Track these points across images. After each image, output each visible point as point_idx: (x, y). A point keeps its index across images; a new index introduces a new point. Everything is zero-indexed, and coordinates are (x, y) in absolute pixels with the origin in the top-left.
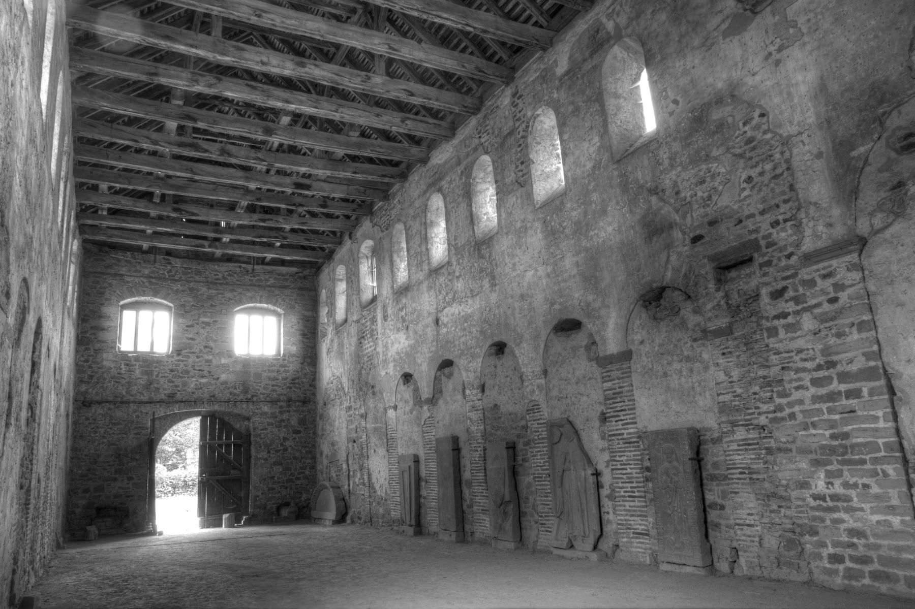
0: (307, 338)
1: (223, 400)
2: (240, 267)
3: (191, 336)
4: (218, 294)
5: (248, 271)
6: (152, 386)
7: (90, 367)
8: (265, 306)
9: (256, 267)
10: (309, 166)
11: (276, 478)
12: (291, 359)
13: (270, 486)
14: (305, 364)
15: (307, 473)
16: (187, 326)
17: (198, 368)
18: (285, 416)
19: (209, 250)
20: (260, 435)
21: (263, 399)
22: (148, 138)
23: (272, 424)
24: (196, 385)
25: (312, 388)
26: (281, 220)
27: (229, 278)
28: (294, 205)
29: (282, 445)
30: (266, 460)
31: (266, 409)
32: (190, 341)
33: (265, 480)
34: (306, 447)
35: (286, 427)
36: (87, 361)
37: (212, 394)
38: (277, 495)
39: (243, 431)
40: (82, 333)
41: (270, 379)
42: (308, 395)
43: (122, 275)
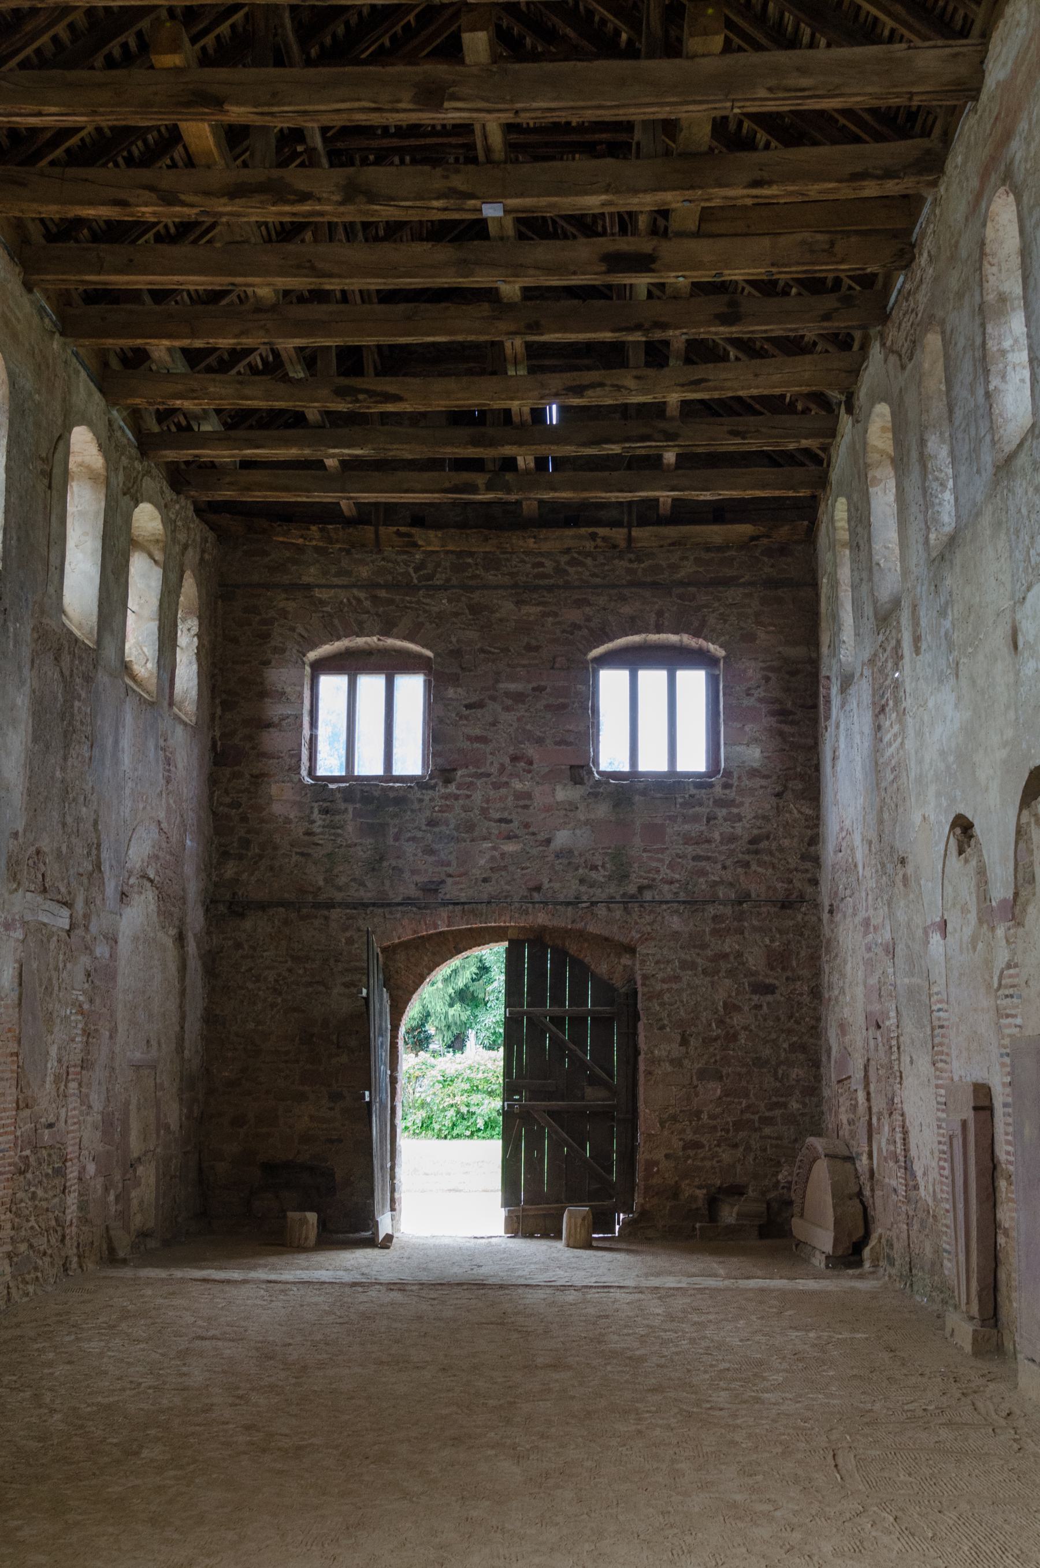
0: (792, 723)
1: (561, 898)
2: (593, 536)
3: (478, 732)
4: (544, 615)
5: (615, 547)
6: (385, 864)
7: (244, 819)
8: (673, 638)
9: (636, 532)
10: (606, 191)
12: (746, 783)
13: (689, 1136)
14: (789, 795)
15: (794, 1105)
16: (468, 707)
17: (498, 816)
18: (729, 944)
19: (490, 496)
20: (660, 994)
21: (669, 897)
22: (151, 188)
23: (693, 966)
24: (493, 858)
25: (808, 865)
26: (630, 383)
27: (571, 570)
28: (638, 327)
29: (721, 1022)
30: (676, 1062)
31: (675, 923)
32: (476, 745)
33: (674, 1118)
34: (790, 1032)
35: (731, 973)
36: (235, 805)
37: (531, 884)
38: (708, 1164)
39: (618, 982)
40: (223, 735)
41: (688, 840)
42: (798, 884)
43: (308, 587)
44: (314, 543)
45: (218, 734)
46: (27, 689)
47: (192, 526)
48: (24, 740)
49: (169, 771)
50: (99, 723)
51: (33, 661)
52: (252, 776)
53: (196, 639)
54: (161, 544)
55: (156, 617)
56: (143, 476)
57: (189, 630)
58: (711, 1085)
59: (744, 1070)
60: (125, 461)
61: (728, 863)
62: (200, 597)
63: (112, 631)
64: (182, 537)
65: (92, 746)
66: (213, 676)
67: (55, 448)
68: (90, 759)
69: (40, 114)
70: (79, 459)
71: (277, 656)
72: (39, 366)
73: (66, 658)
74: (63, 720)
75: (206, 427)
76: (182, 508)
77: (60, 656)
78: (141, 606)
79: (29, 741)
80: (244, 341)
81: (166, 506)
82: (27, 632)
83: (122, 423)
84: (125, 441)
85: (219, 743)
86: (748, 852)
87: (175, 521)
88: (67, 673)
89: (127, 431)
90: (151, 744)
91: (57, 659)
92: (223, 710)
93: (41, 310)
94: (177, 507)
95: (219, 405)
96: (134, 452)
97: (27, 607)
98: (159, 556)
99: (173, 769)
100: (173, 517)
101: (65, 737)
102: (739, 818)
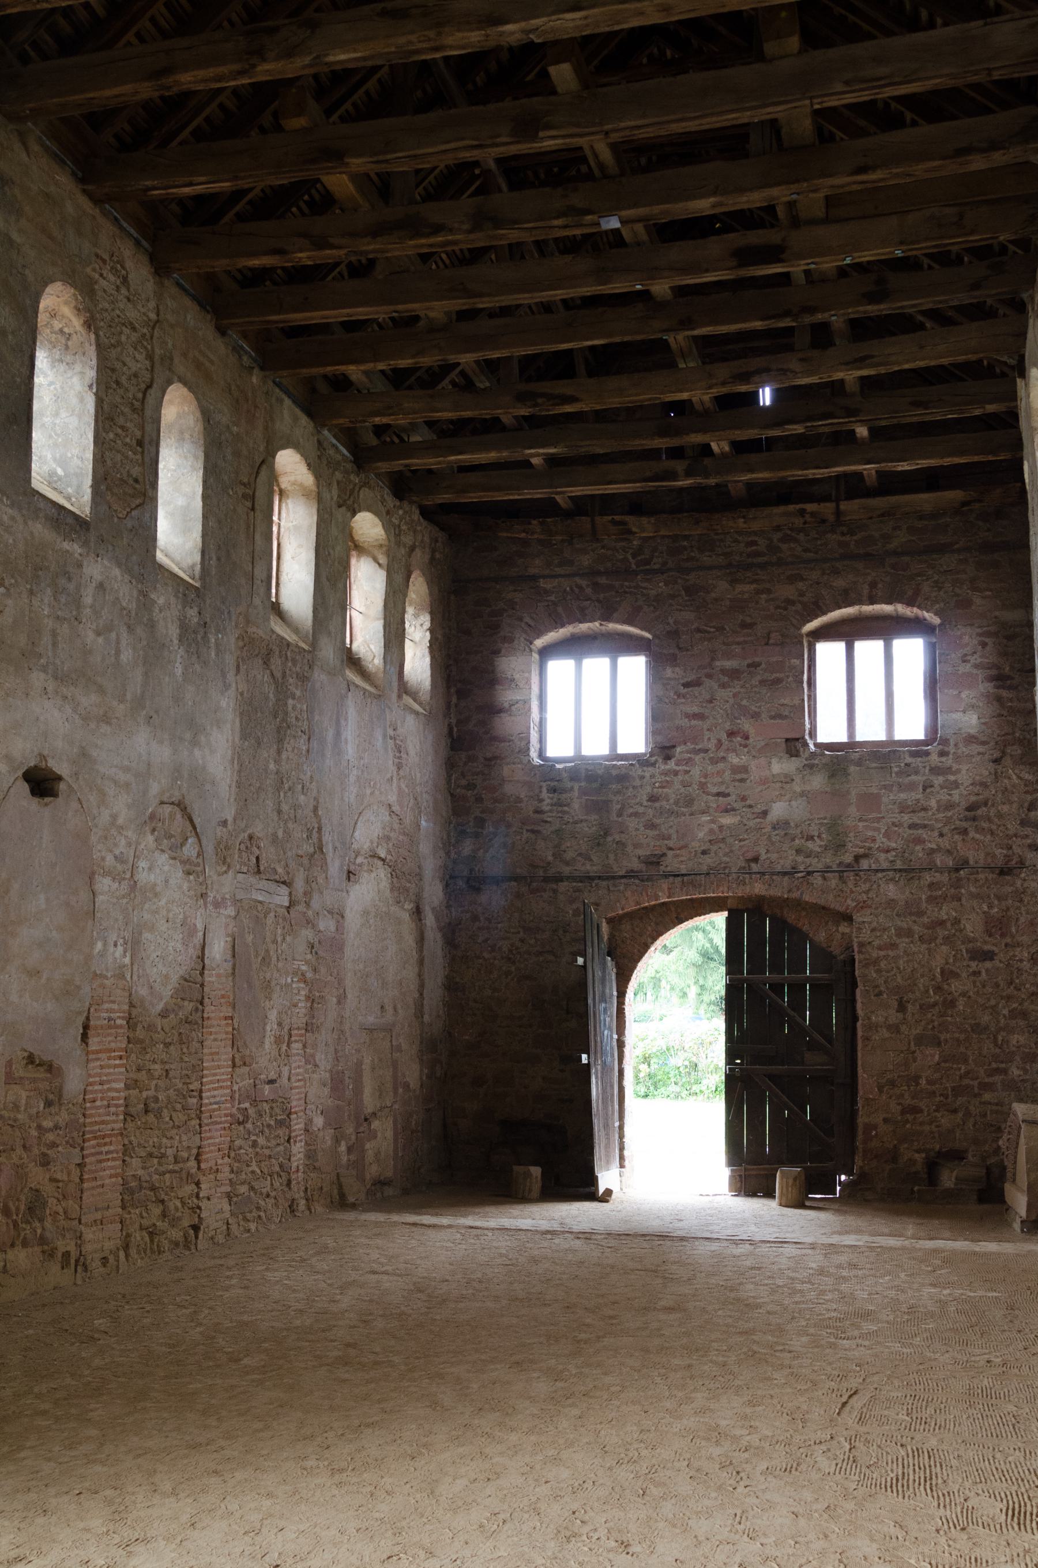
0: (1010, 688)
1: (778, 868)
2: (802, 512)
3: (696, 709)
4: (758, 592)
5: (823, 521)
6: (609, 839)
7: (479, 799)
8: (887, 608)
9: (844, 506)
10: (714, 193)
11: (923, 1082)
12: (963, 749)
13: (908, 1101)
14: (1007, 761)
15: (1015, 1072)
16: (686, 685)
17: (715, 790)
18: (946, 912)
19: (689, 482)
20: (876, 962)
21: (885, 865)
23: (909, 933)
24: (711, 831)
26: (794, 365)
27: (784, 547)
28: (787, 314)
29: (938, 989)
30: (895, 1029)
31: (891, 891)
32: (694, 722)
33: (892, 1083)
35: (947, 940)
36: (471, 786)
37: (750, 855)
38: (927, 1128)
39: (836, 949)
40: (459, 722)
41: (903, 808)
42: (1017, 850)
43: (534, 578)
44: (536, 536)
45: (454, 721)
46: (232, 693)
47: (419, 528)
48: (230, 738)
49: (400, 758)
50: (317, 718)
51: (238, 667)
52: (486, 759)
53: (428, 634)
54: (384, 549)
55: (381, 615)
56: (360, 489)
57: (422, 625)
58: (929, 1051)
59: (962, 1036)
60: (338, 475)
61: (945, 830)
62: (431, 594)
63: (330, 633)
64: (408, 539)
65: (309, 739)
66: (448, 667)
67: (258, 473)
68: (308, 751)
69: (191, 184)
70: (292, 478)
71: (506, 645)
72: (237, 400)
73: (276, 662)
74: (275, 718)
75: (415, 438)
76: (405, 512)
77: (269, 660)
78: (367, 607)
79: (237, 740)
80: (422, 360)
81: (388, 513)
82: (231, 640)
83: (334, 441)
84: (340, 458)
85: (455, 729)
86: (966, 819)
87: (399, 526)
88: (278, 675)
89: (341, 448)
90: (378, 734)
91: (266, 663)
92: (458, 699)
93: (236, 349)
94: (401, 512)
95: (413, 419)
96: (349, 466)
97: (230, 619)
98: (383, 560)
99: (404, 756)
100: (397, 522)
101: (279, 732)
102: (956, 785)
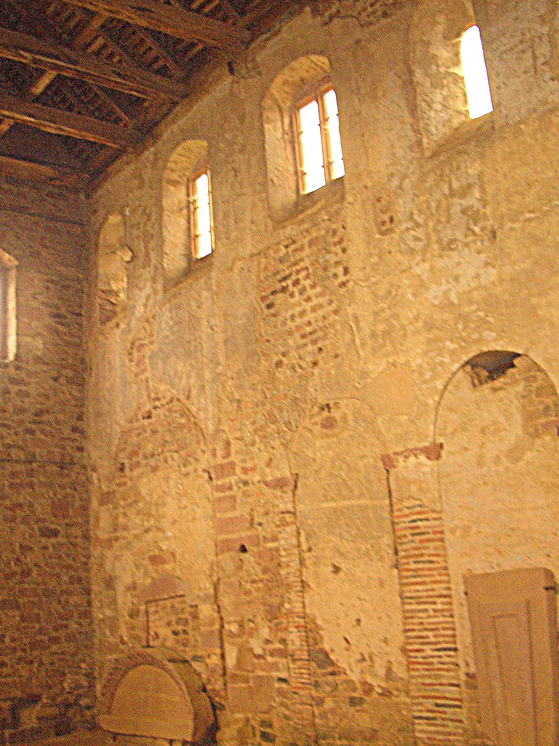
11: (7, 640)
15: (74, 626)
25: (77, 436)
34: (68, 567)
35: (25, 520)
58: (11, 613)
59: (35, 600)
61: (20, 430)
86: (35, 422)
102: (27, 395)
